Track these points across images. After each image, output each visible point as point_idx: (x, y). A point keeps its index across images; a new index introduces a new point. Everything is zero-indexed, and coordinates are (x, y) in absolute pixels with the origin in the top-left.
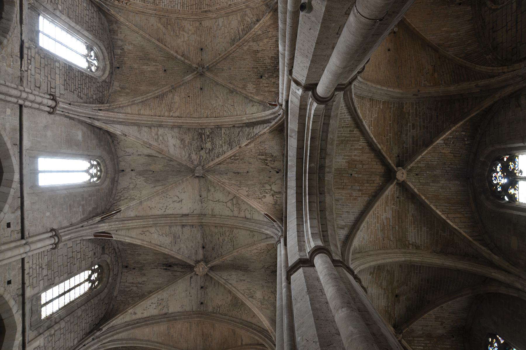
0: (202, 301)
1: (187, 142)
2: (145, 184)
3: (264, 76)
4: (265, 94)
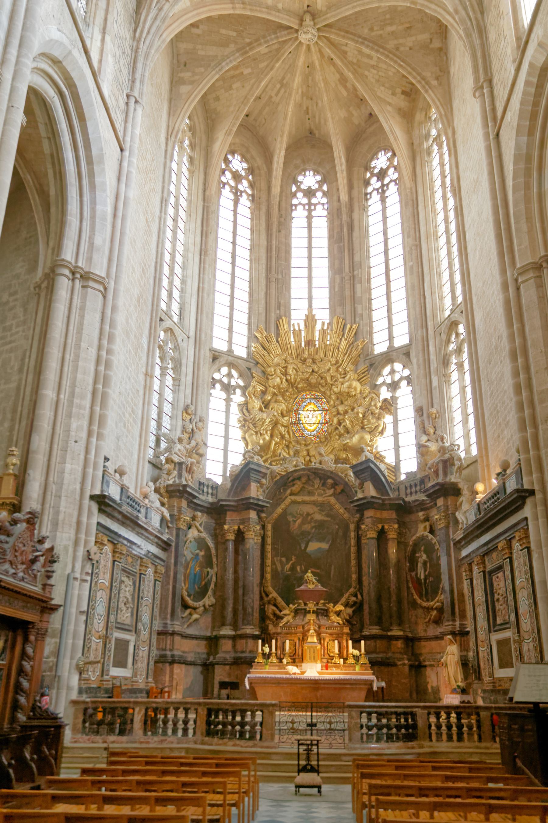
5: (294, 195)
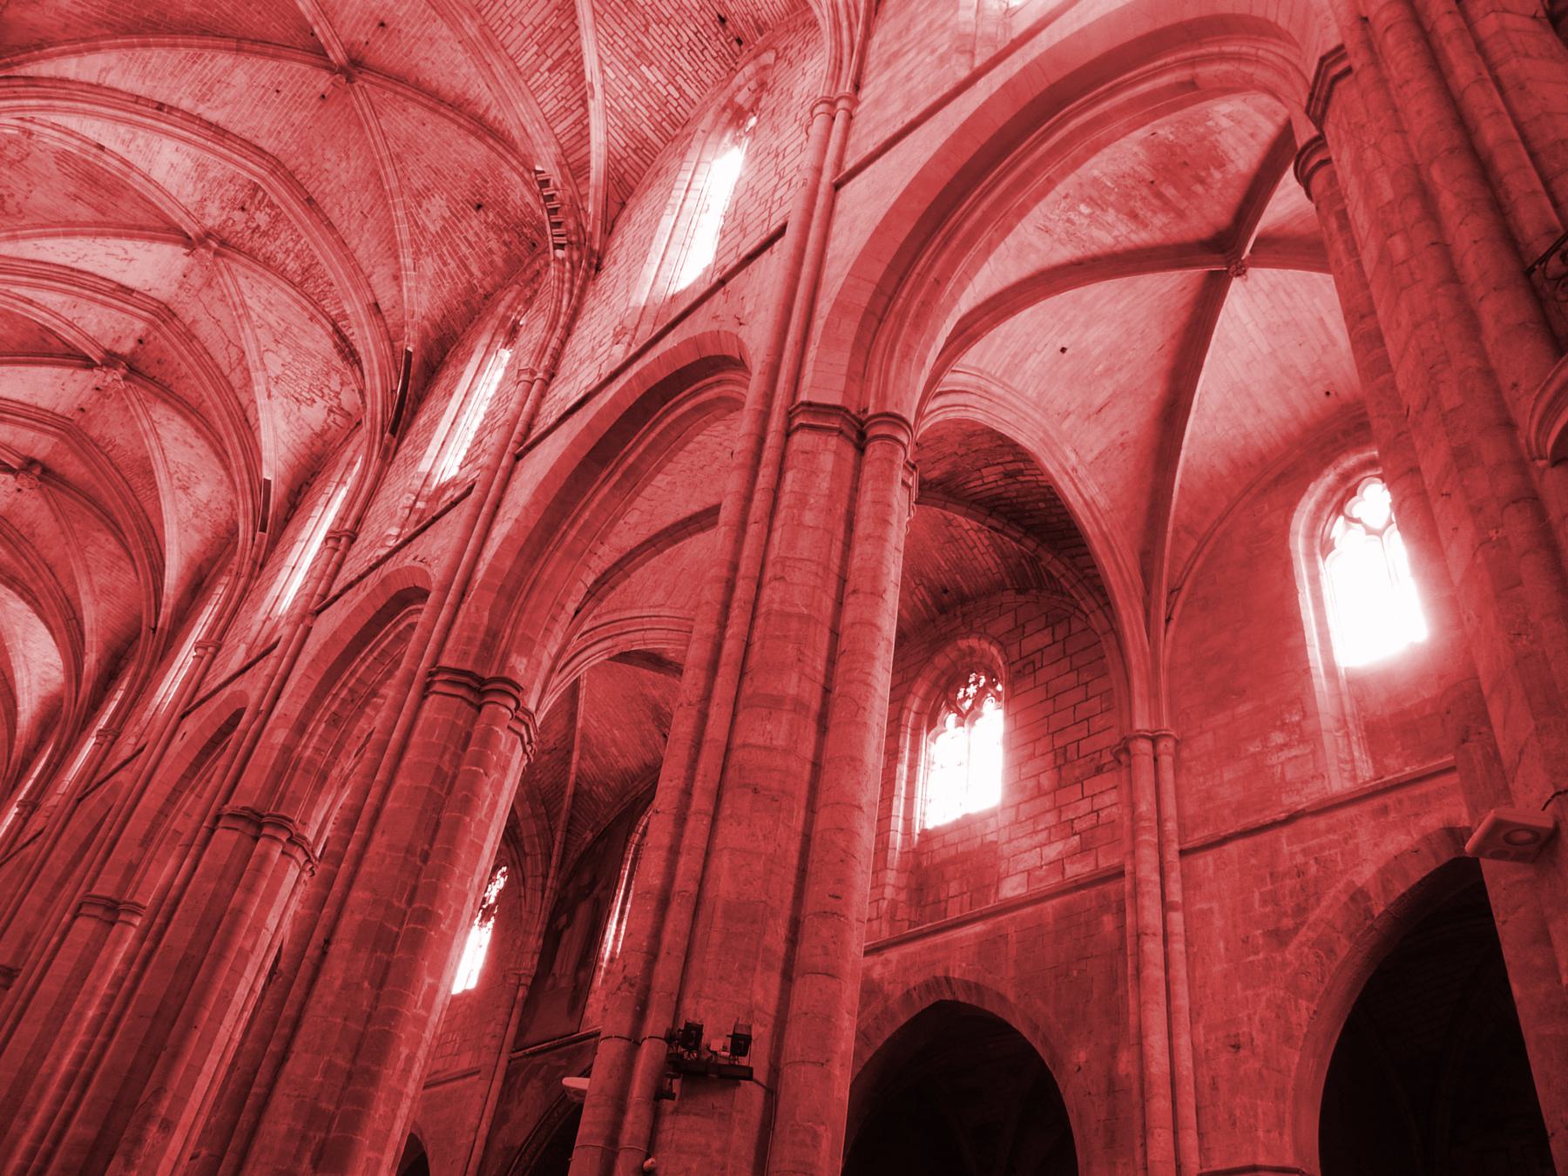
0: (85, 407)
1: (211, 175)
2: (54, 167)
4: (449, 261)
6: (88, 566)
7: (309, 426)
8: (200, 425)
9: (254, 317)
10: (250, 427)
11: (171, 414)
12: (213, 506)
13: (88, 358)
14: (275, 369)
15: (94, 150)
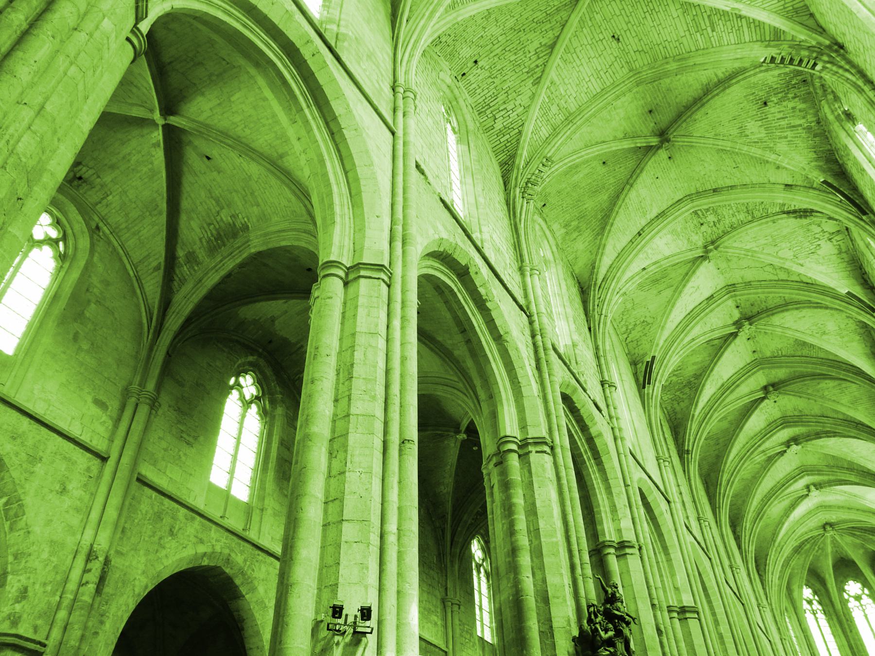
1: (679, 230)
3: (771, 101)
4: (785, 134)
5: (848, 601)
6: (834, 401)
7: (831, 255)
8: (795, 306)
9: (757, 249)
10: (812, 284)
11: (781, 315)
12: (843, 326)
13: (732, 334)
14: (789, 254)
15: (644, 272)
